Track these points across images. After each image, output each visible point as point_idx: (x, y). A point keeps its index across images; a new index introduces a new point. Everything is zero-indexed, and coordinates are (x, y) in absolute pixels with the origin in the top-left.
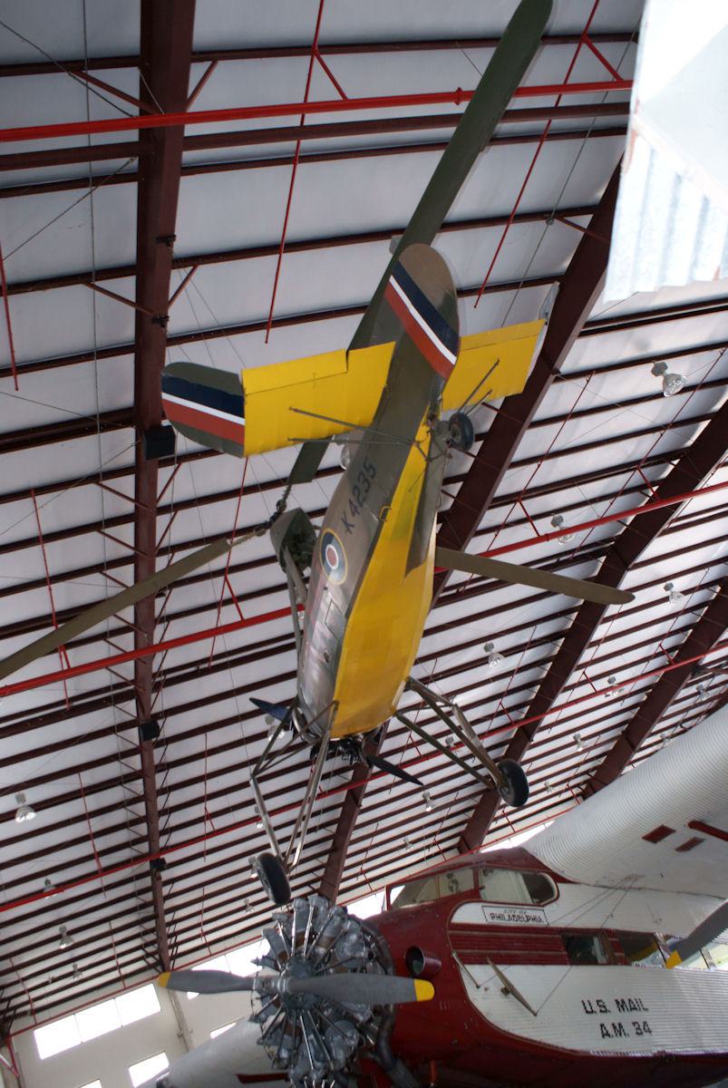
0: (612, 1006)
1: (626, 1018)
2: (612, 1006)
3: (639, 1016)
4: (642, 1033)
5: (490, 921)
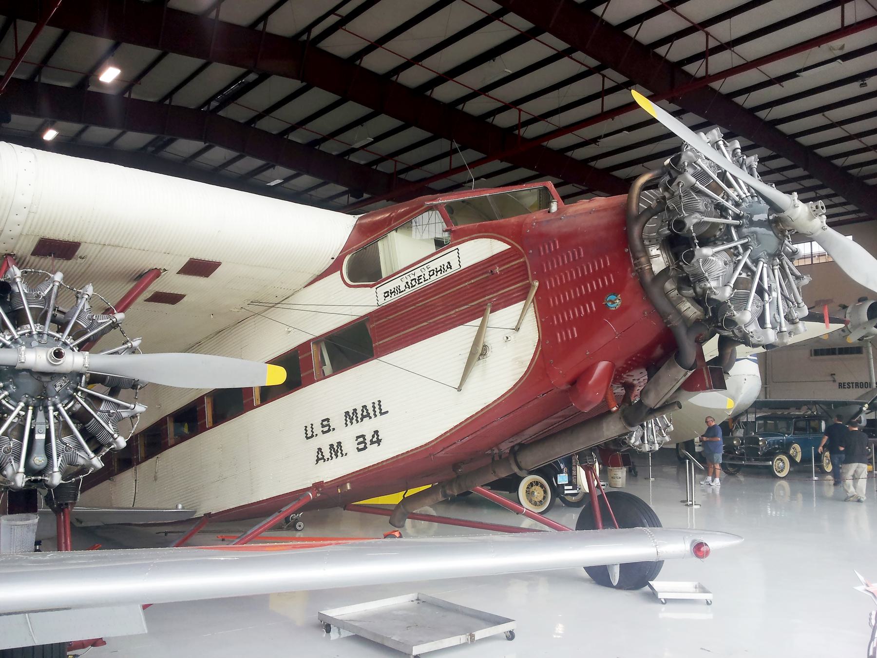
0: (337, 421)
1: (347, 435)
3: (366, 427)
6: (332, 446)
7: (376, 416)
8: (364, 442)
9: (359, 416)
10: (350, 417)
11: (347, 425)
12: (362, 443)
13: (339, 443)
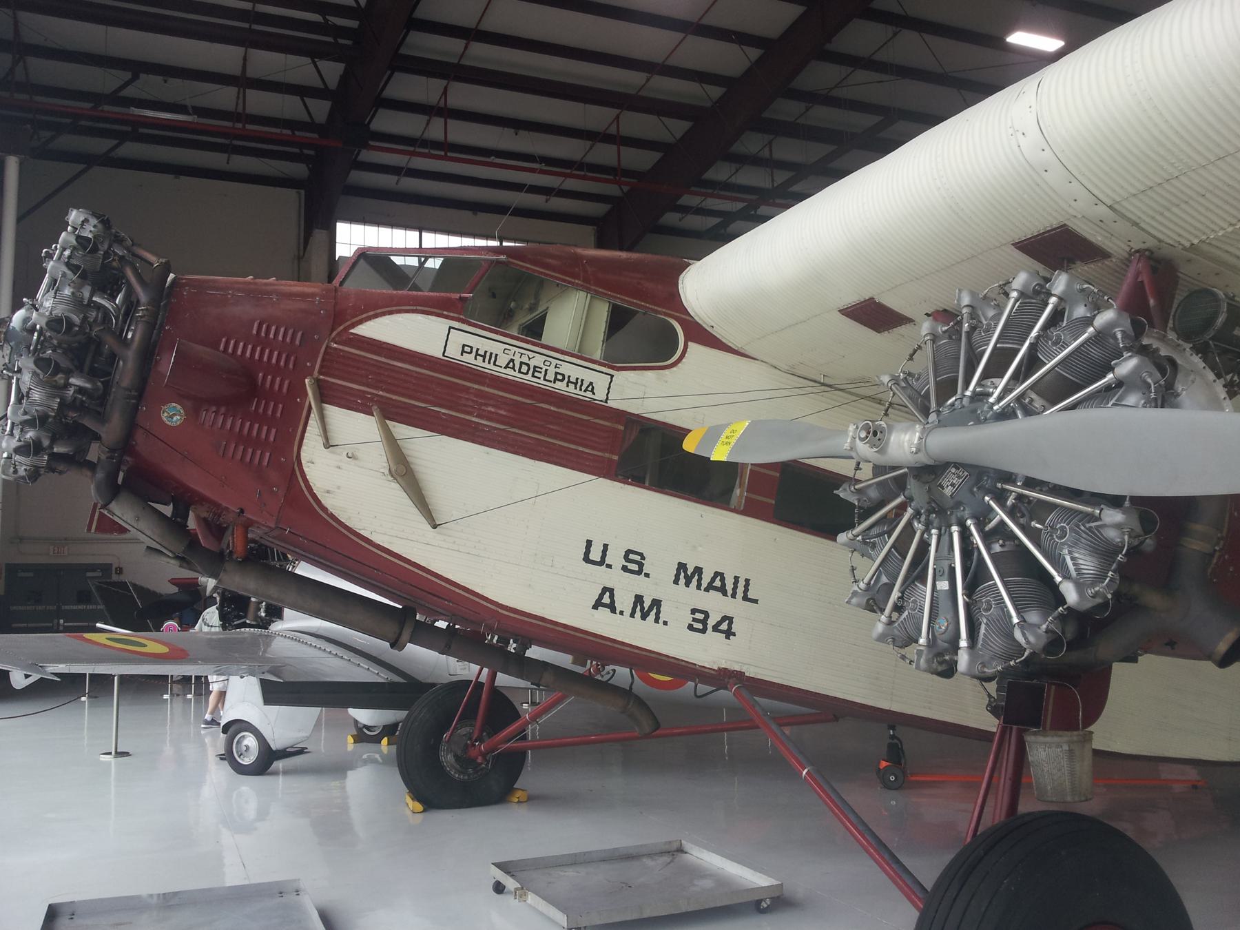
0: (661, 568)
1: (680, 602)
2: (661, 568)
4: (704, 631)
5: (454, 352)
6: (639, 599)
7: (734, 596)
8: (704, 622)
9: (704, 584)
10: (685, 574)
11: (676, 582)
12: (700, 622)
13: (656, 603)
